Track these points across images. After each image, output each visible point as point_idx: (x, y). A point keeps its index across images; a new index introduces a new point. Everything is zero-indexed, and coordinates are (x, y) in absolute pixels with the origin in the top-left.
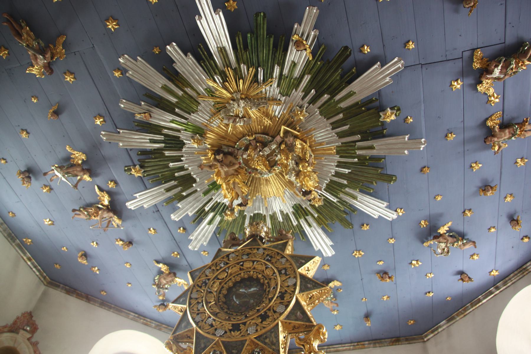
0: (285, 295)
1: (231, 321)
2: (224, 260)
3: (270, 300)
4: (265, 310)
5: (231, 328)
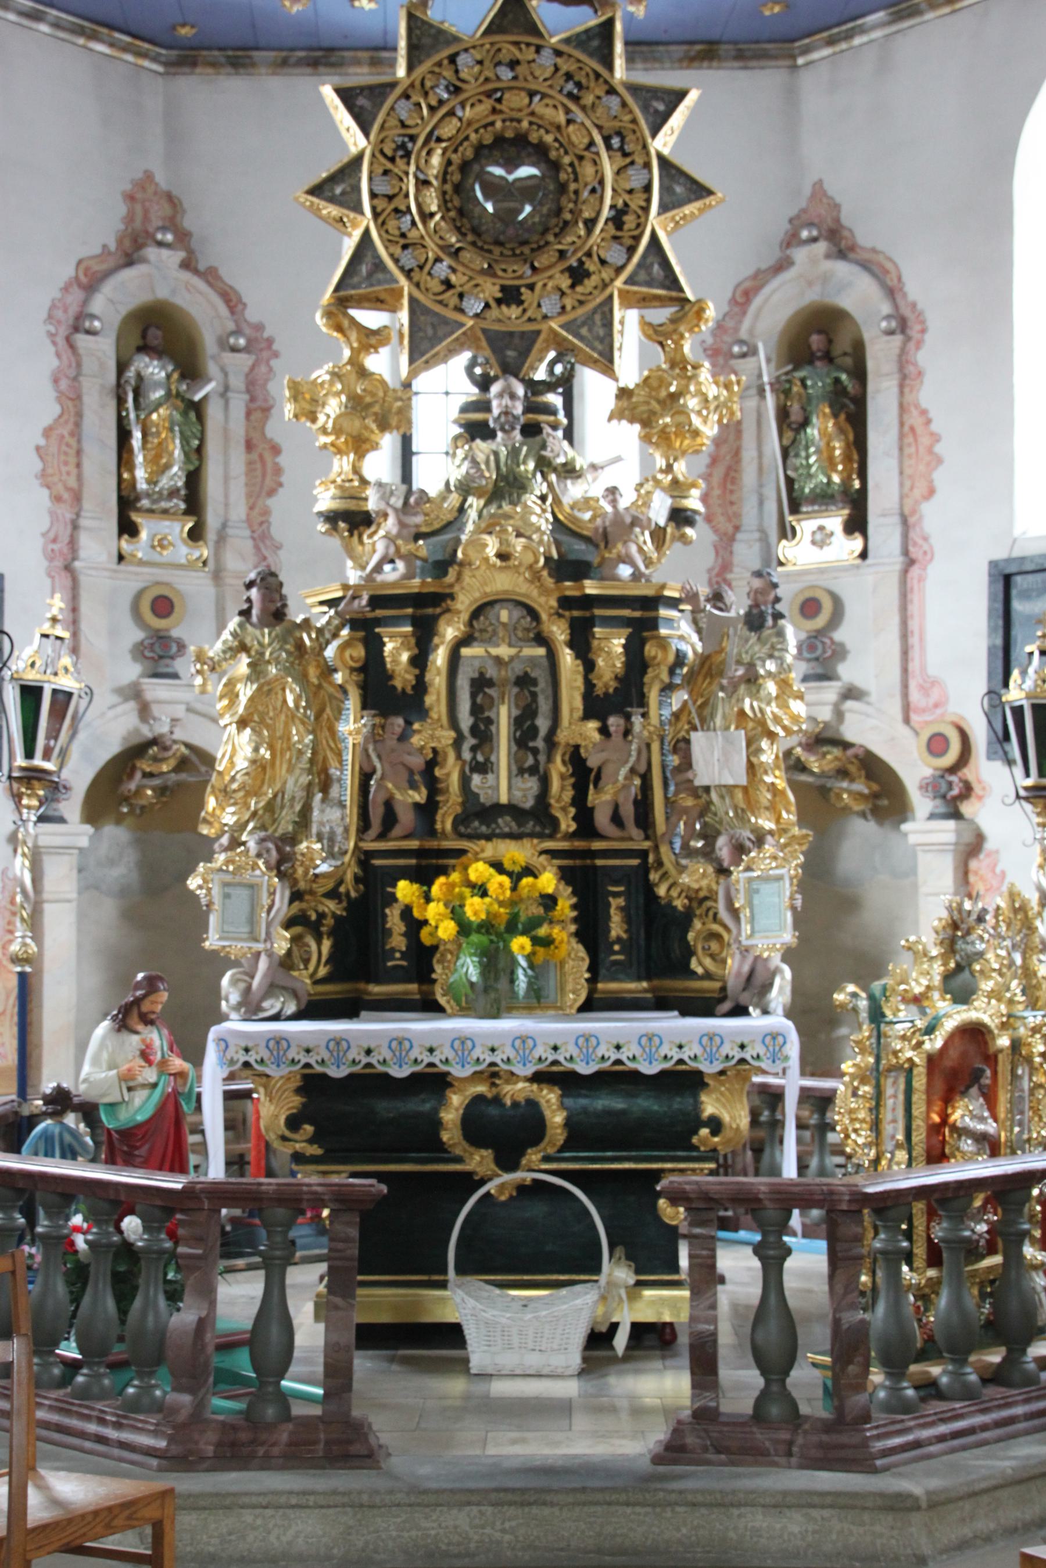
0: (626, 218)
1: (494, 275)
2: (446, 73)
3: (590, 224)
4: (580, 254)
5: (499, 295)
